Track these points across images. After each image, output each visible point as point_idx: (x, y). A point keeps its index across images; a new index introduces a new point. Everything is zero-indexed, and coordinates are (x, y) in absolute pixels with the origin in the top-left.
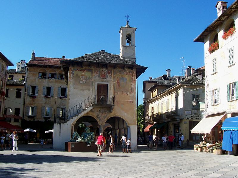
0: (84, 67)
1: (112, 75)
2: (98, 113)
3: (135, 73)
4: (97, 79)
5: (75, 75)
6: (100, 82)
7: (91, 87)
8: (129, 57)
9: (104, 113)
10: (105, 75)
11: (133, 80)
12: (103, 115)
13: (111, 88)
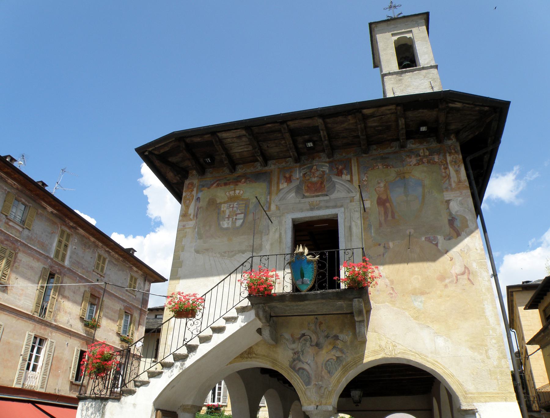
0: (240, 170)
1: (355, 178)
2: (297, 346)
3: (456, 152)
4: (290, 204)
5: (203, 204)
6: (302, 210)
7: (264, 238)
10: (322, 183)
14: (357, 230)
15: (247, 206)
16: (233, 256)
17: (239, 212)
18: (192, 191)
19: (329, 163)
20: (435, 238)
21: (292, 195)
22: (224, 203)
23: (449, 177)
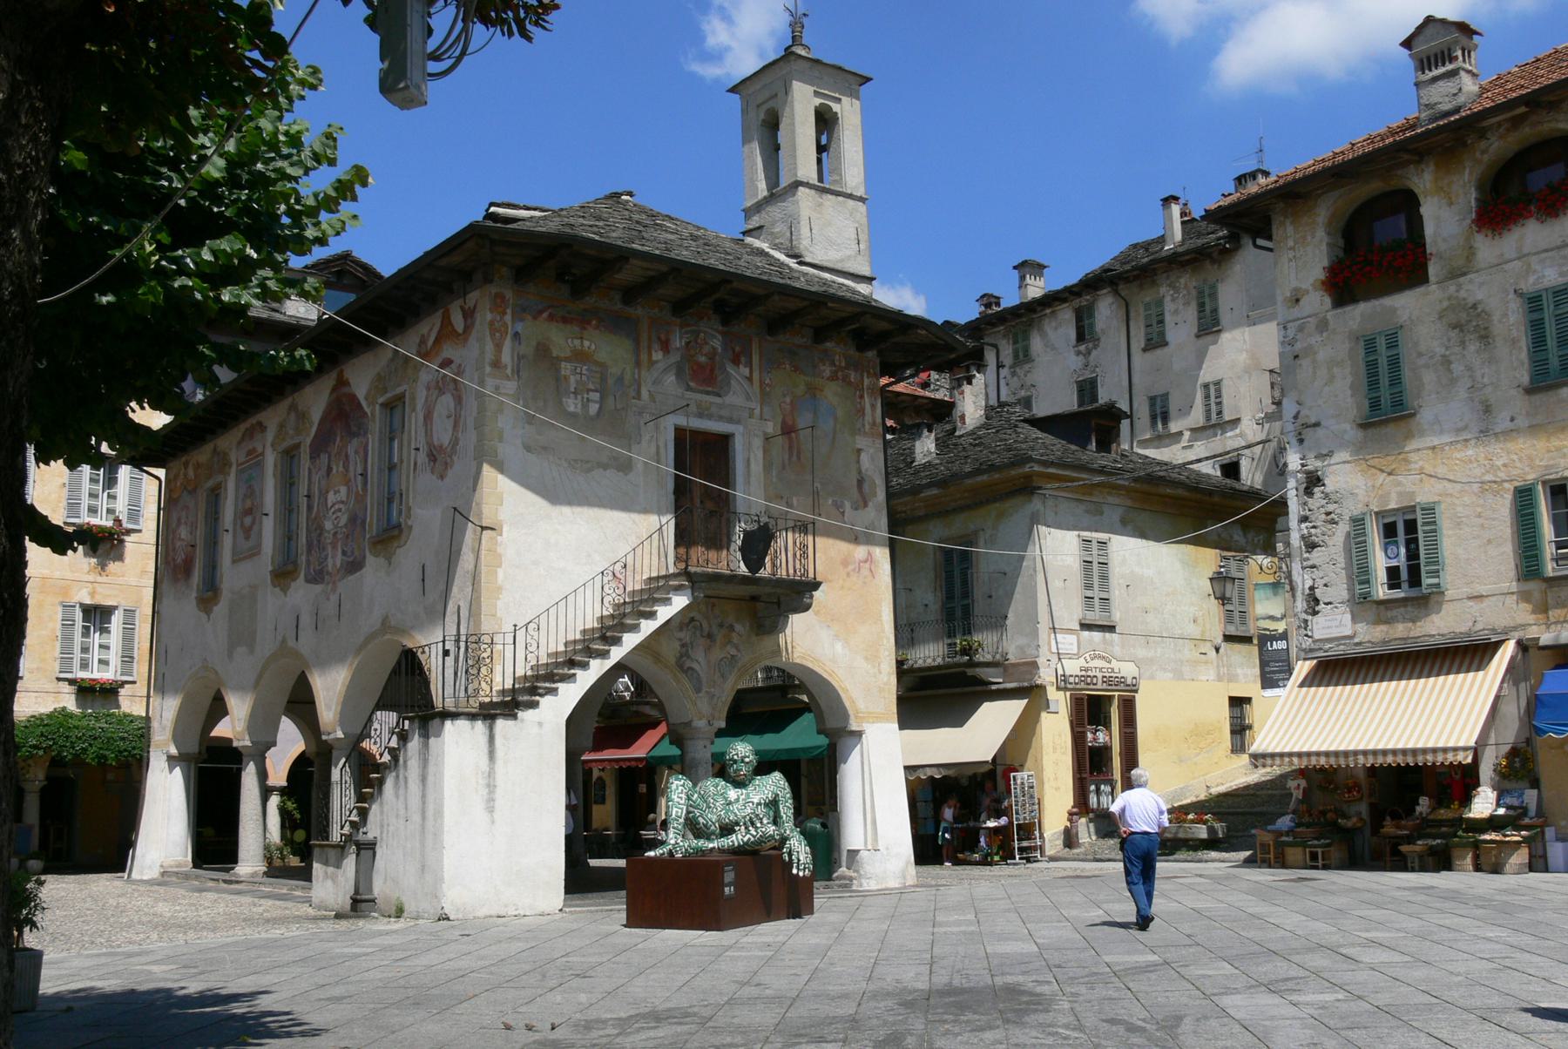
0: (590, 301)
1: (756, 376)
2: (685, 635)
5: (527, 348)
8: (839, 266)
9: (719, 638)
10: (712, 370)
11: (868, 418)
12: (717, 654)
13: (753, 466)
14: (757, 467)
15: (603, 379)
16: (589, 470)
17: (591, 386)
18: (504, 313)
19: (723, 334)
20: (842, 505)
21: (671, 379)
22: (567, 359)
23: (862, 412)
